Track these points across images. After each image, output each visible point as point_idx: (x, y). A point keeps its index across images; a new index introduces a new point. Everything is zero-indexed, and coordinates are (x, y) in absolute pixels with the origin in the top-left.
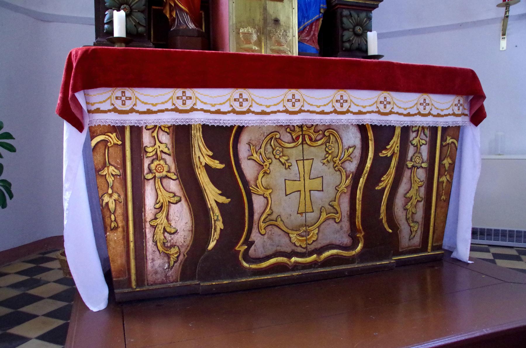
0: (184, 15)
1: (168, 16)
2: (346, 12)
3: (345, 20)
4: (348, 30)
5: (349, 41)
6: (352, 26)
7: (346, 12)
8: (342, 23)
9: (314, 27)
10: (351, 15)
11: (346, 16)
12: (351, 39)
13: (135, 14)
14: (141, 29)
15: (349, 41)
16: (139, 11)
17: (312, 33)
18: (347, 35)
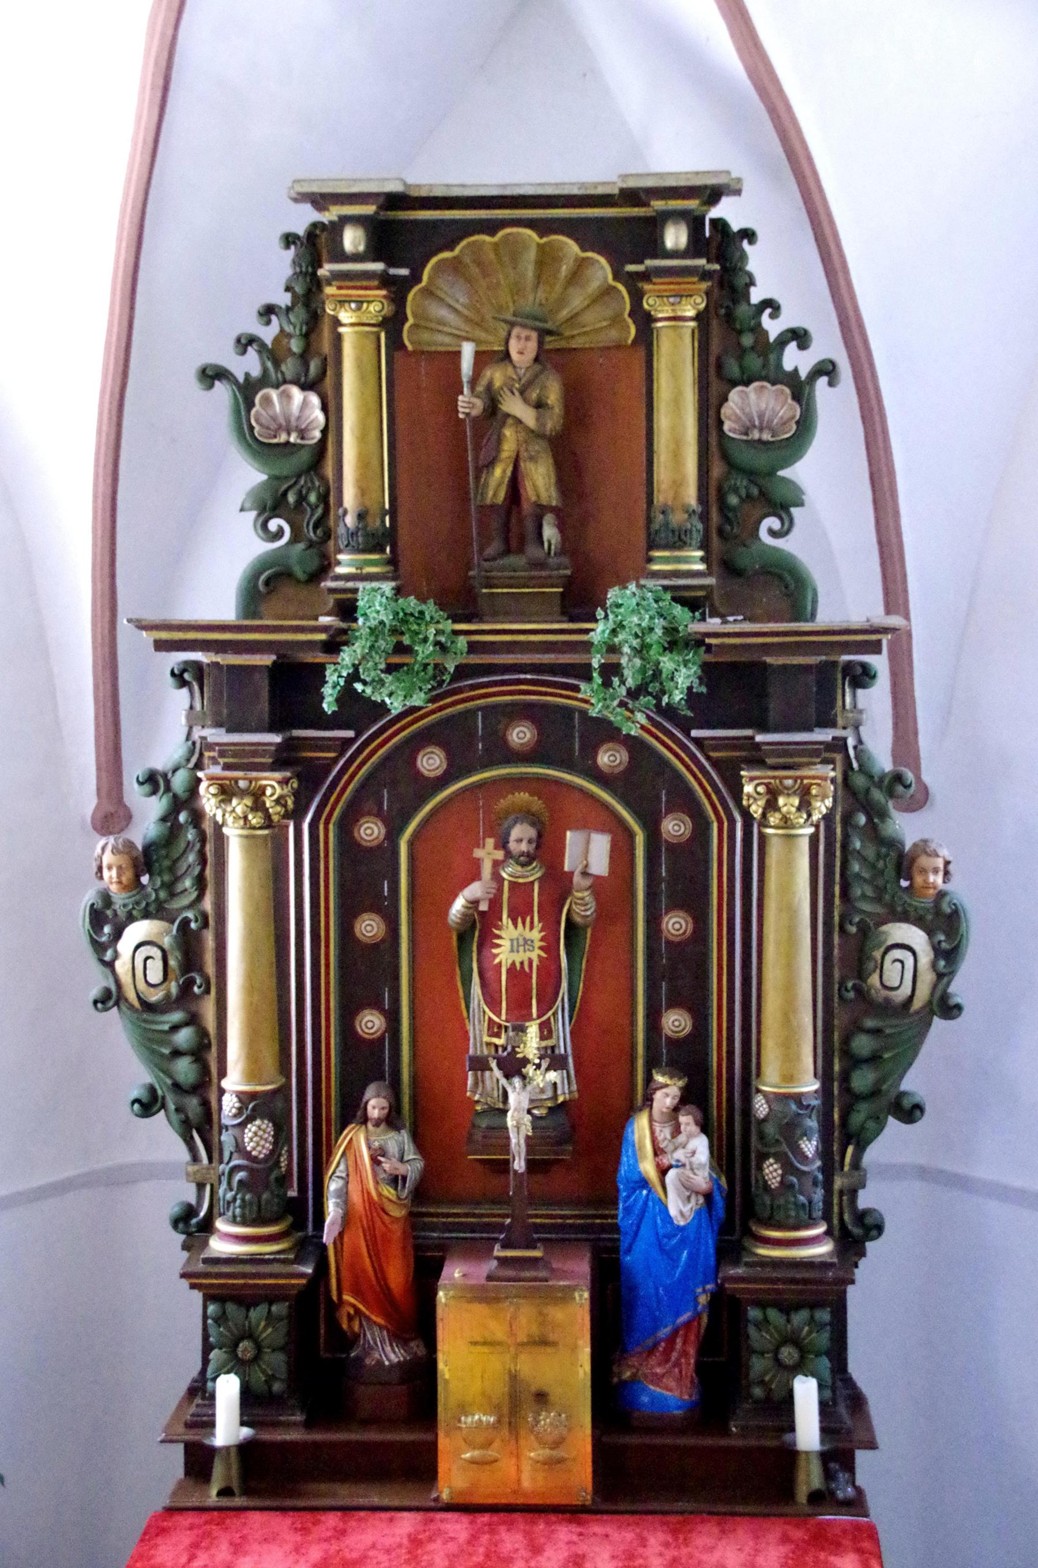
0: (376, 1329)
1: (345, 1326)
2: (754, 1313)
3: (752, 1331)
4: (762, 1354)
5: (762, 1383)
6: (771, 1347)
7: (754, 1313)
8: (748, 1337)
9: (679, 1341)
10: (766, 1320)
11: (758, 1325)
12: (767, 1378)
13: (266, 1358)
14: (277, 1387)
15: (762, 1383)
16: (274, 1350)
17: (674, 1355)
18: (758, 1365)
